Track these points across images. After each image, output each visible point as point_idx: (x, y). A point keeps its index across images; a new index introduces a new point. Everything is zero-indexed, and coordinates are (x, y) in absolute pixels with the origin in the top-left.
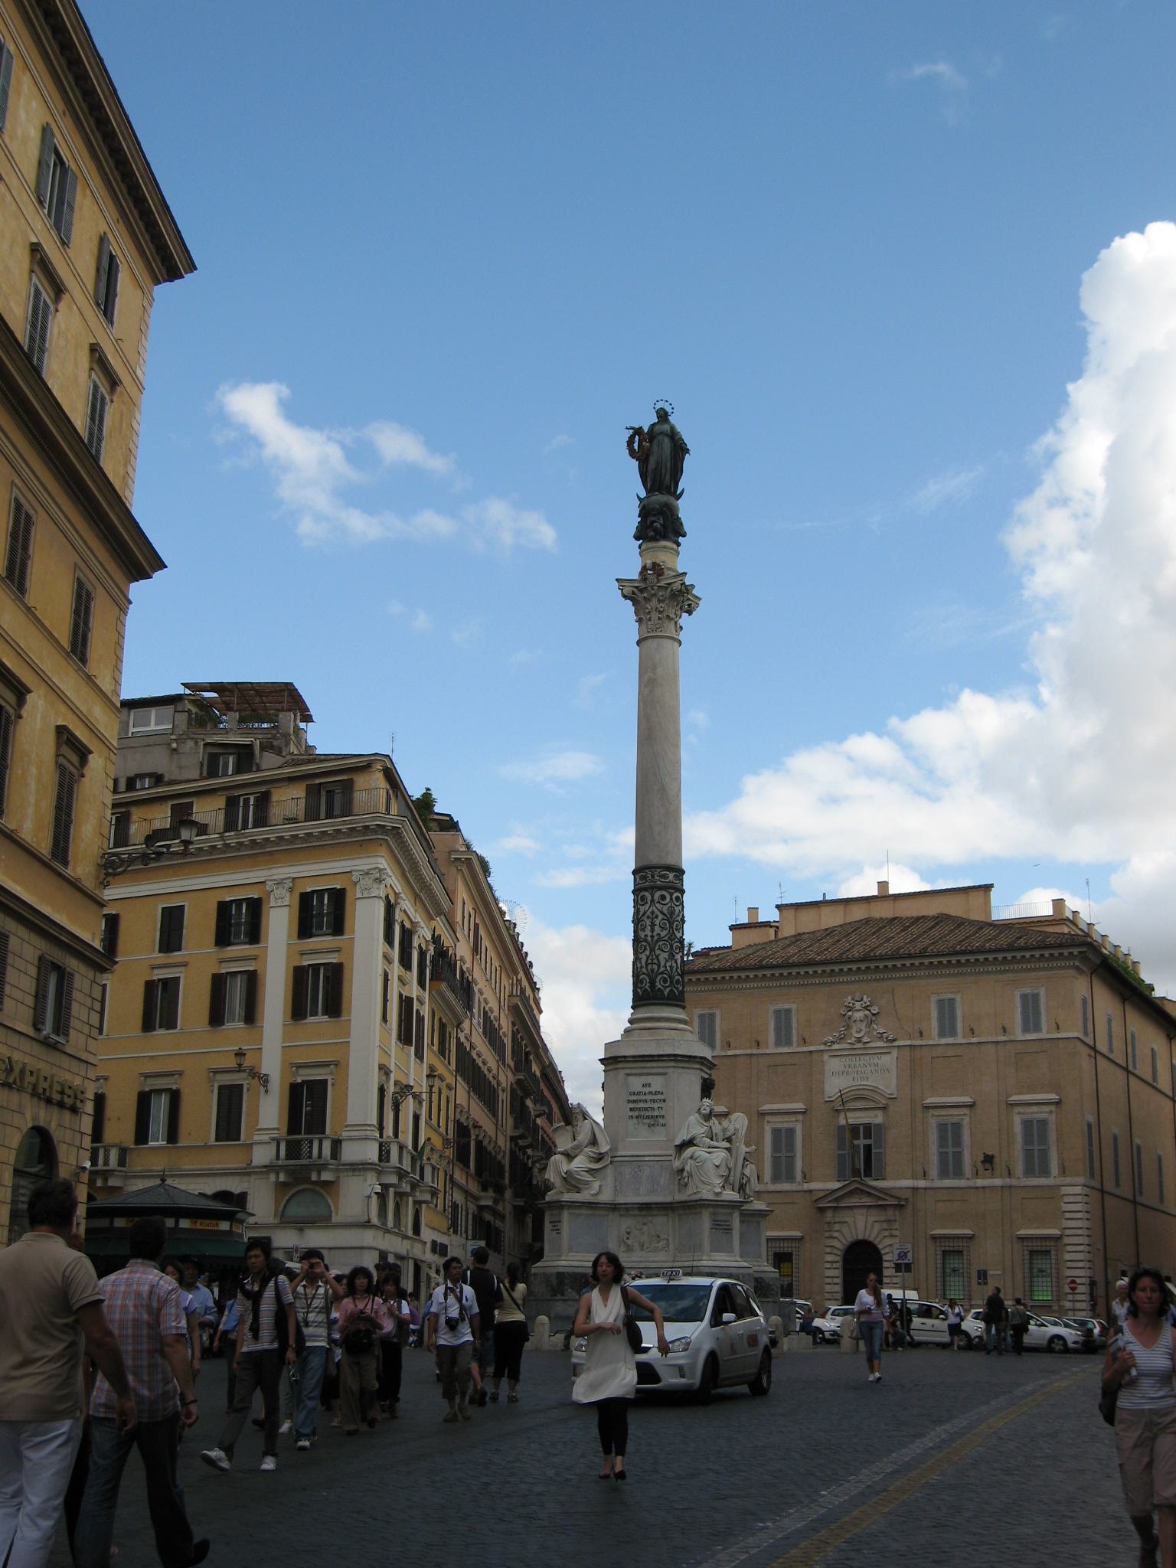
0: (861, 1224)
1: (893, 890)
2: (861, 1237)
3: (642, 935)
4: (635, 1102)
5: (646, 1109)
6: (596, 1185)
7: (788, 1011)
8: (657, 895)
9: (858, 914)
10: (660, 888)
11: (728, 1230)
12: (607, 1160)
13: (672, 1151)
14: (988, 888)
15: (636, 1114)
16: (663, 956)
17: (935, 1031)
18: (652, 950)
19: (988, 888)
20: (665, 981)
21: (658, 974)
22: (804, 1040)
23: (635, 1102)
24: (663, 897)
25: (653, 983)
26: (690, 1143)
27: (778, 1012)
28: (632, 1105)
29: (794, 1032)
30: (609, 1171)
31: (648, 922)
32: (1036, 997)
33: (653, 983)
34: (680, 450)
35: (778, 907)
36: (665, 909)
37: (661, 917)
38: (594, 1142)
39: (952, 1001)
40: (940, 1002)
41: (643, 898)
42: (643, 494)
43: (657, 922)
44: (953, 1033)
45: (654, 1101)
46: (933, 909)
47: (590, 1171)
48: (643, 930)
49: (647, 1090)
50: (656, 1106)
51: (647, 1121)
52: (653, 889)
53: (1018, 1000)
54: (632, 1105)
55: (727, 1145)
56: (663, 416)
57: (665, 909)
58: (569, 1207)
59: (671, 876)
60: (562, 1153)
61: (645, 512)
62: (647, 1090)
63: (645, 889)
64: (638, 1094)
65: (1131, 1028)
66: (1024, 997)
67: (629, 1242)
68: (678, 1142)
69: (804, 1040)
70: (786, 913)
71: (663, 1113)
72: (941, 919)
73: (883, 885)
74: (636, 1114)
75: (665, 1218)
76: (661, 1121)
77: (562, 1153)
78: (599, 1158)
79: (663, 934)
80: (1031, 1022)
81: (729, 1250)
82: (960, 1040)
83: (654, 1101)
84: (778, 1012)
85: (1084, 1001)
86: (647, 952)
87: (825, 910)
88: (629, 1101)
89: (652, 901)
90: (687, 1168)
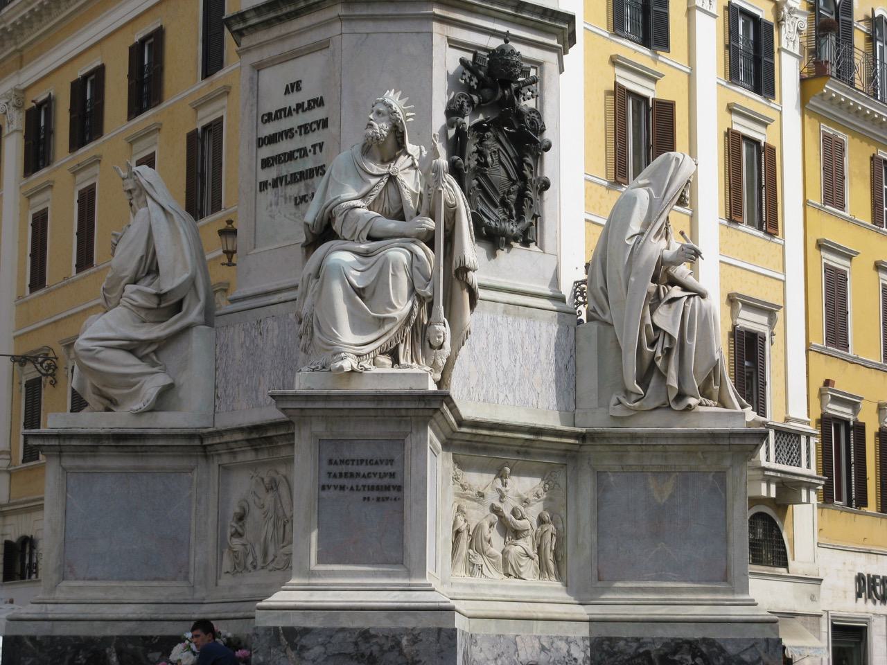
4: (272, 139)
5: (290, 156)
6: (151, 387)
12: (193, 313)
15: (270, 174)
23: (272, 139)
28: (267, 151)
30: (198, 342)
38: (149, 268)
45: (306, 129)
47: (133, 348)
49: (293, 100)
54: (267, 151)
58: (60, 453)
74: (270, 174)
78: (168, 306)
83: (306, 129)
88: (262, 142)
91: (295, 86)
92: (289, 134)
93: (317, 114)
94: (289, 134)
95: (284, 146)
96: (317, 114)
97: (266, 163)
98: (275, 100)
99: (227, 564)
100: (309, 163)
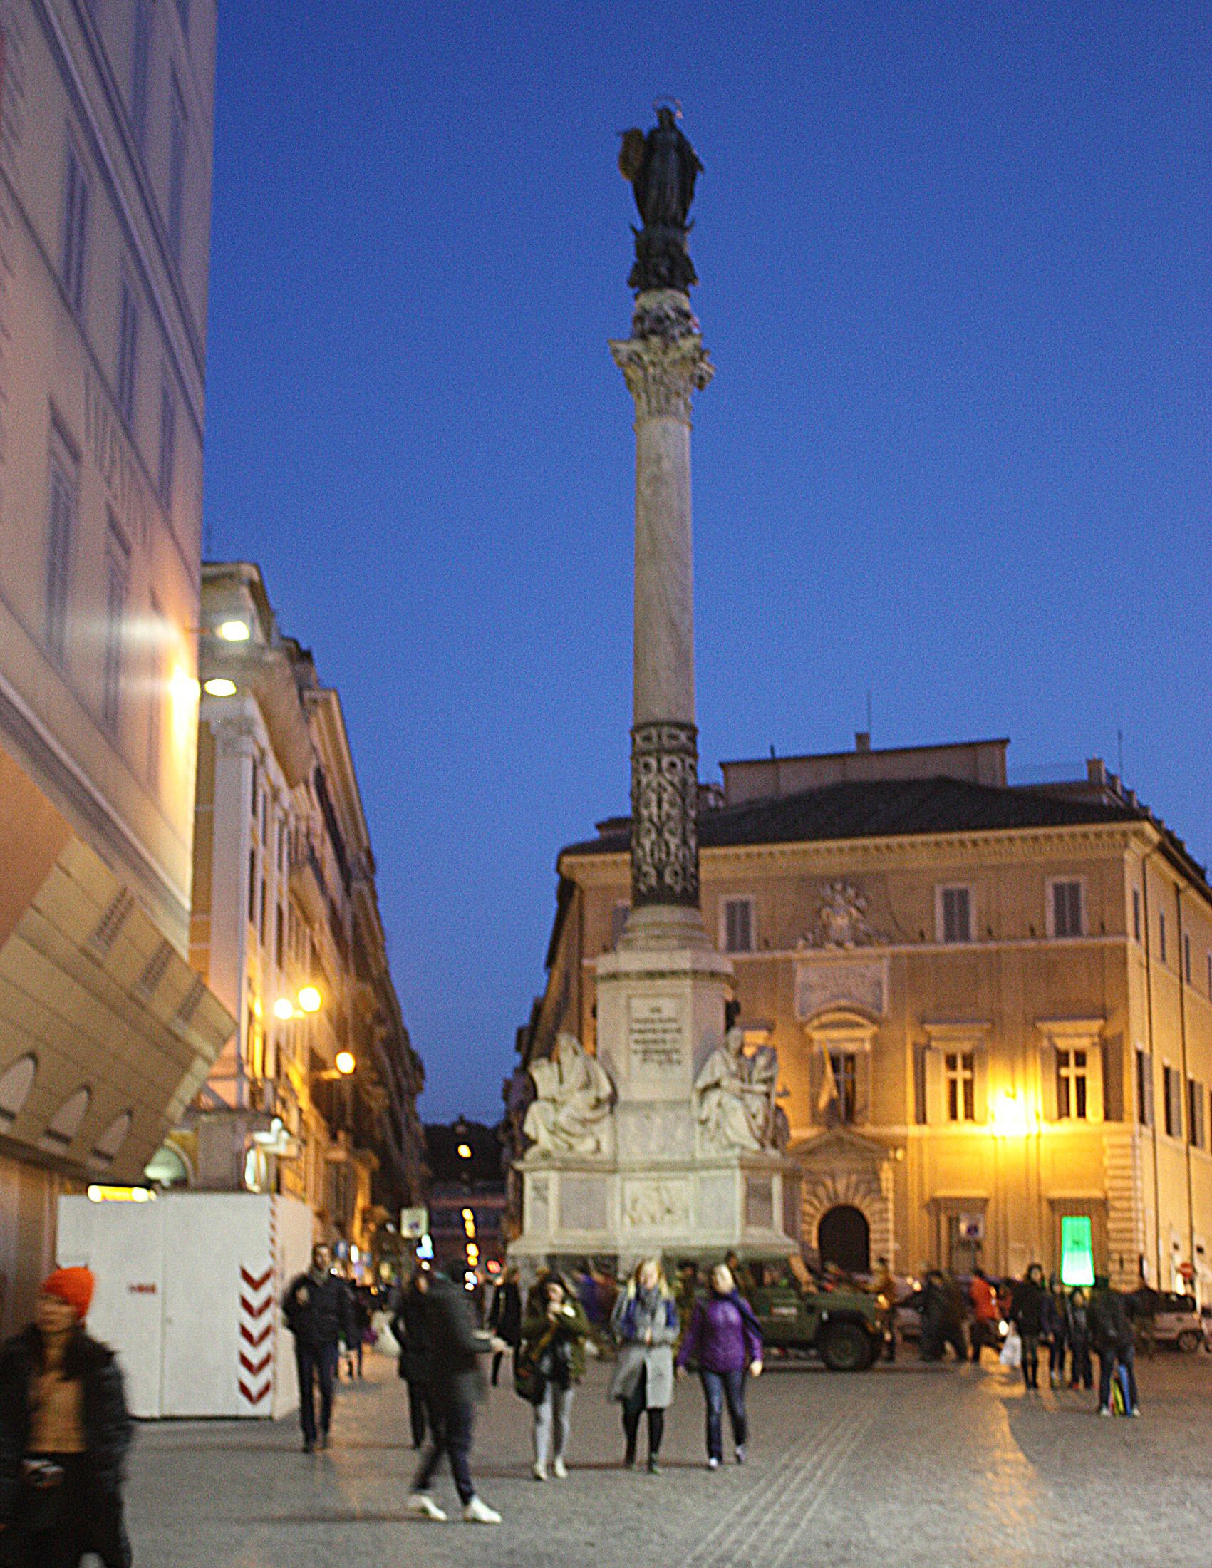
0: (841, 1187)
1: (875, 745)
2: (841, 1201)
3: (645, 813)
4: (641, 1031)
5: (655, 1042)
7: (745, 906)
8: (665, 761)
9: (830, 775)
10: (670, 752)
11: (768, 1198)
13: (695, 1099)
14: (1005, 742)
16: (674, 842)
17: (940, 933)
18: (659, 832)
19: (1005, 742)
20: (676, 873)
21: (664, 867)
22: (766, 942)
23: (641, 1031)
24: (673, 765)
25: (660, 875)
26: (717, 1085)
27: (731, 907)
28: (636, 1036)
29: (753, 934)
31: (654, 797)
32: (1074, 888)
33: (660, 875)
34: (690, 167)
35: (723, 765)
36: (676, 780)
37: (670, 789)
39: (963, 895)
40: (948, 895)
41: (647, 766)
42: (639, 225)
43: (665, 796)
44: (966, 937)
45: (665, 1031)
46: (930, 768)
47: (584, 1122)
48: (647, 806)
50: (668, 1037)
51: (656, 1057)
52: (660, 751)
53: (1050, 892)
55: (762, 1088)
56: (666, 116)
57: (676, 780)
59: (683, 736)
60: (547, 1099)
61: (644, 248)
62: (656, 1016)
63: (649, 753)
64: (646, 1021)
65: (1185, 930)
66: (1058, 889)
67: (635, 1215)
68: (700, 1084)
69: (766, 942)
70: (732, 772)
71: (677, 1046)
72: (943, 782)
73: (862, 738)
74: (640, 1047)
75: (681, 1183)
76: (675, 1057)
77: (547, 1099)
79: (674, 812)
80: (1068, 923)
81: (768, 1223)
82: (974, 946)
83: (665, 1031)
84: (731, 907)
85: (1136, 895)
86: (653, 836)
87: (785, 771)
88: (632, 1031)
89: (660, 769)
90: (713, 1118)
91: (658, 1010)
92: (654, 1031)
93: (674, 1026)
94: (654, 1031)
95: (650, 1036)
96: (674, 1026)
97: (637, 1042)
98: (646, 1014)
99: (627, 1220)
100: (668, 1047)
